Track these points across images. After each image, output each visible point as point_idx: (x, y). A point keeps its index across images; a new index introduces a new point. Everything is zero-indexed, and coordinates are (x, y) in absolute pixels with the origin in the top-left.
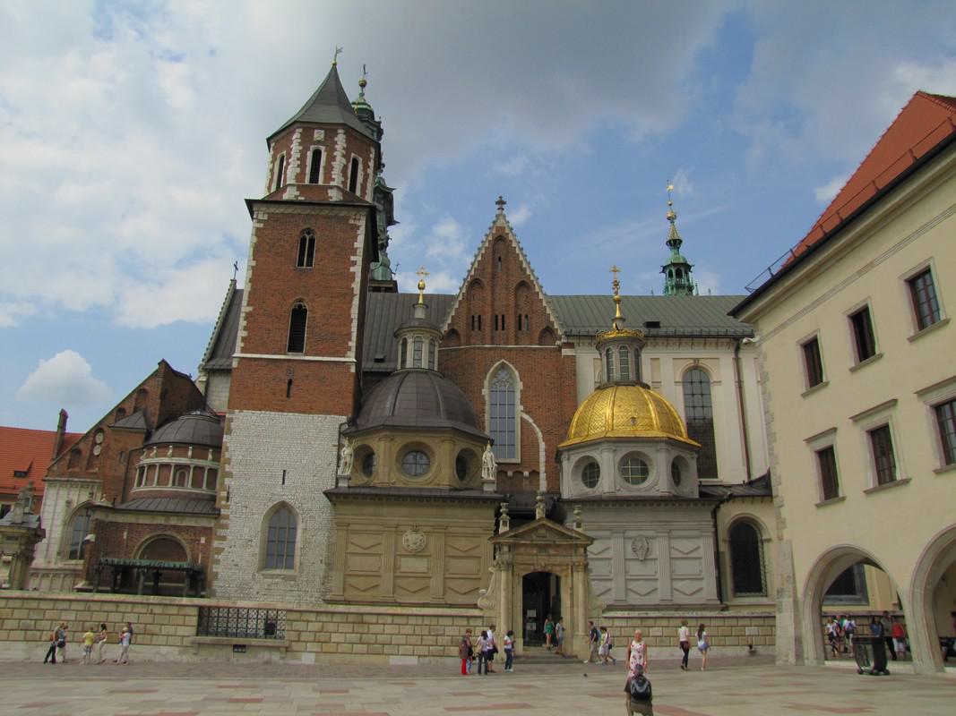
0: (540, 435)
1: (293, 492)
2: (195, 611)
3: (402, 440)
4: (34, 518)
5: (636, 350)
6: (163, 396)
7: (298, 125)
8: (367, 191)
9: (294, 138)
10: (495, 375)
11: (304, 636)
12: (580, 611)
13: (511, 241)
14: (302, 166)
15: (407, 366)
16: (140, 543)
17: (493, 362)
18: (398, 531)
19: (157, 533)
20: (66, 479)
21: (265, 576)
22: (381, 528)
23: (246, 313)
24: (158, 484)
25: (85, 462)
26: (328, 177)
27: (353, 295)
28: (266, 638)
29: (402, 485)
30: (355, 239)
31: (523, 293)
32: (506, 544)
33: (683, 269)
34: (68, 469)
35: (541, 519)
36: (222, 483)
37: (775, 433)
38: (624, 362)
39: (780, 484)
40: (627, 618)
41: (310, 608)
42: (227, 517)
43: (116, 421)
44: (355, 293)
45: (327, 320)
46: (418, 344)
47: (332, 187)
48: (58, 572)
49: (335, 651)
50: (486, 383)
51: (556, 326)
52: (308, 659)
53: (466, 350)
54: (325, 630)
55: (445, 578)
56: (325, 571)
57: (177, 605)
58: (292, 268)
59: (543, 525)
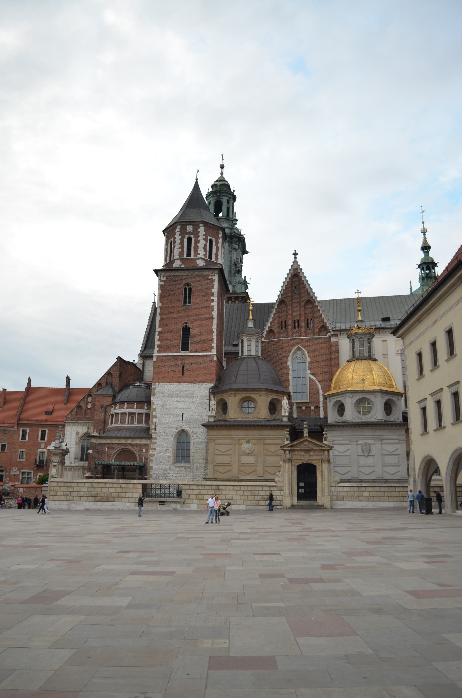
0: (320, 386)
2: (141, 486)
4: (63, 444)
5: (369, 339)
6: (120, 376)
7: (178, 224)
8: (219, 257)
9: (176, 231)
10: (295, 353)
11: (192, 497)
12: (326, 483)
14: (182, 247)
15: (244, 355)
17: (293, 347)
18: (239, 442)
19: (120, 448)
20: (75, 421)
21: (176, 467)
23: (159, 332)
24: (121, 423)
25: (84, 412)
26: (196, 253)
27: (213, 318)
28: (178, 498)
29: (241, 419)
31: (309, 306)
32: (287, 450)
33: (431, 266)
34: (76, 415)
35: (306, 436)
36: (152, 421)
37: (409, 397)
41: (194, 483)
42: (156, 438)
43: (97, 391)
44: (214, 317)
46: (249, 343)
47: (198, 259)
48: (76, 468)
50: (290, 359)
51: (328, 325)
53: (278, 341)
54: (201, 494)
56: (205, 464)
57: (132, 484)
58: (180, 306)
59: (306, 440)
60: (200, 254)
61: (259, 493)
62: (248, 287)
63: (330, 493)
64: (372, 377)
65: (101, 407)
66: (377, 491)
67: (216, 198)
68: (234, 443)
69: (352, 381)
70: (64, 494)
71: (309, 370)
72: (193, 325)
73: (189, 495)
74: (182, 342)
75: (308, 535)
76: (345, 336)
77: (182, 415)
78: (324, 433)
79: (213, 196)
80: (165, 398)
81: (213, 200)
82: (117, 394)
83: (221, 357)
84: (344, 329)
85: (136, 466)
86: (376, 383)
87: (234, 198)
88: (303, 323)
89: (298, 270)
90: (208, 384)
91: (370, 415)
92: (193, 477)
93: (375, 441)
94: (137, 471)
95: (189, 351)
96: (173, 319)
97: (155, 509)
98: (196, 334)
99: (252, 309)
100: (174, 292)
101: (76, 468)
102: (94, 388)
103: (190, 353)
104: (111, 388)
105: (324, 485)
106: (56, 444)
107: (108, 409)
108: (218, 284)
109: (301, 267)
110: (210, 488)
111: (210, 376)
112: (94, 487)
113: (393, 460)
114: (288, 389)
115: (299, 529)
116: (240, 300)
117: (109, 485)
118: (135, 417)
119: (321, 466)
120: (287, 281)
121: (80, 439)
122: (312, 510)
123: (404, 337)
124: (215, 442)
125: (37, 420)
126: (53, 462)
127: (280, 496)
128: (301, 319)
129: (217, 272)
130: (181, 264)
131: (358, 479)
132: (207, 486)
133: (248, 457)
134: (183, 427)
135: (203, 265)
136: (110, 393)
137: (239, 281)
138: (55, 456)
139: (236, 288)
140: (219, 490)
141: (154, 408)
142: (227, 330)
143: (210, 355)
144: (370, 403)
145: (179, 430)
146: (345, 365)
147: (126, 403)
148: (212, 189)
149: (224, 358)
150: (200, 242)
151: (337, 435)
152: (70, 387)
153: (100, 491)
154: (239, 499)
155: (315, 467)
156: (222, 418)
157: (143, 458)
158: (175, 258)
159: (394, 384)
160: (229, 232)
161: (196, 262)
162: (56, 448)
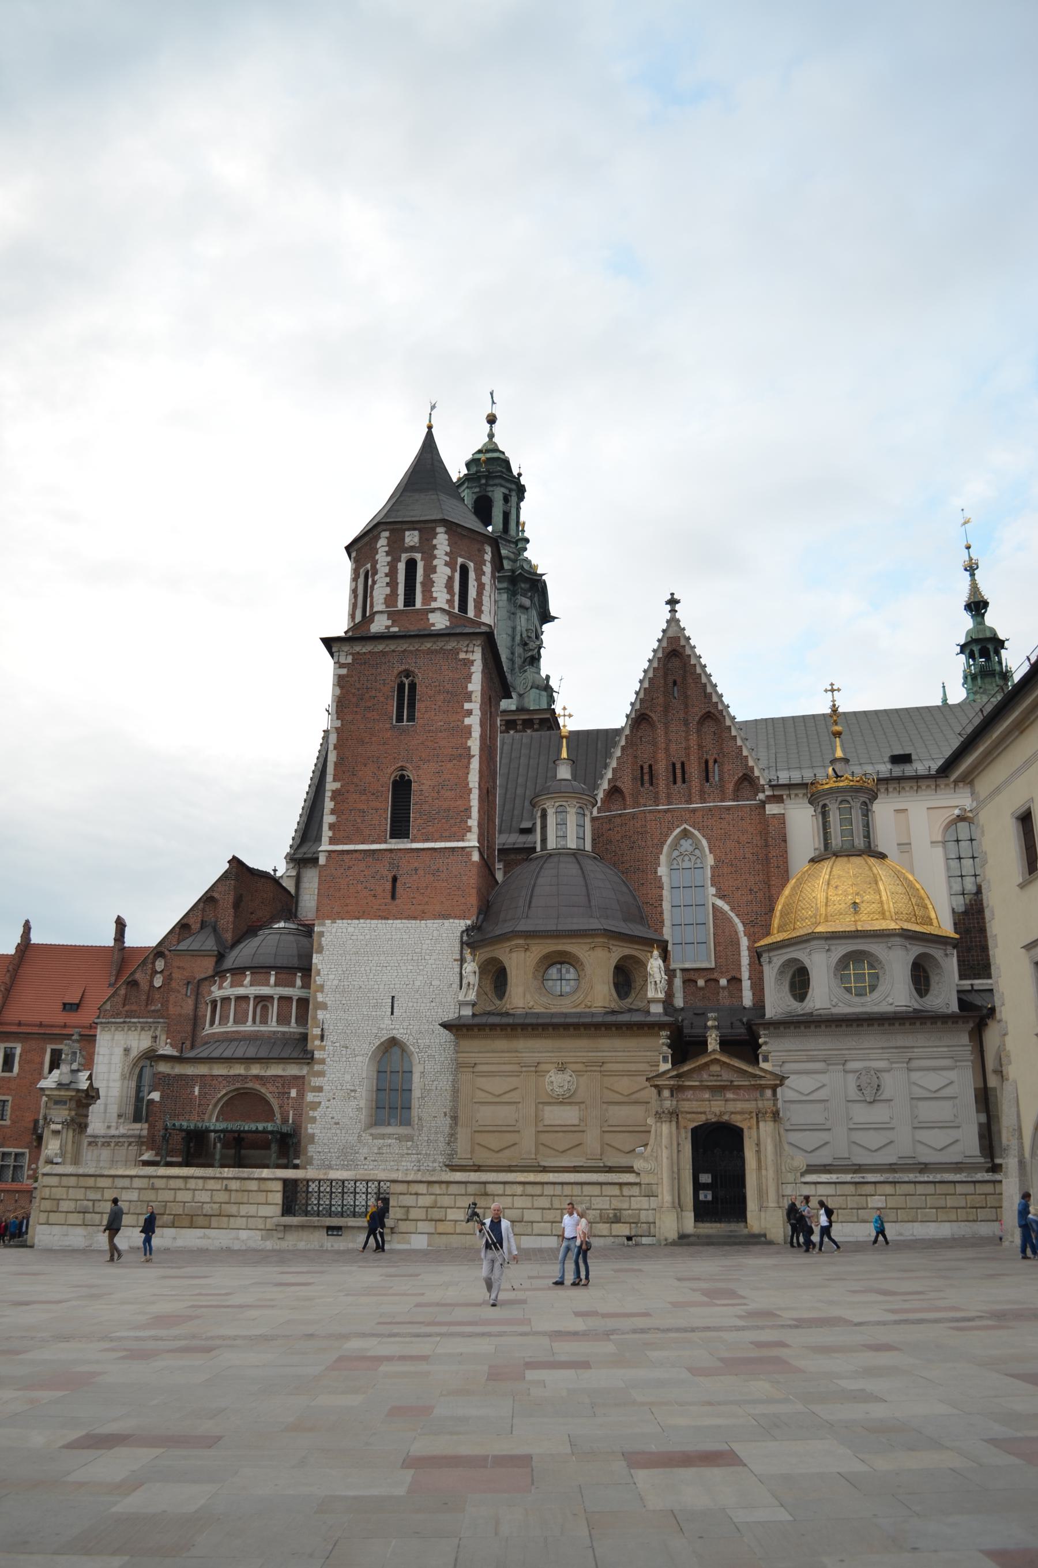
0: (740, 928)
1: (406, 1024)
2: (278, 1186)
3: (540, 949)
4: (84, 1075)
5: (865, 803)
6: (237, 905)
7: (382, 527)
8: (483, 608)
10: (675, 846)
11: (414, 1214)
12: (770, 1174)
13: (689, 656)
14: (393, 584)
17: (671, 830)
18: (538, 1071)
19: (232, 1087)
20: (121, 1020)
21: (374, 1137)
22: (516, 1068)
23: (333, 791)
24: (235, 1022)
25: (144, 997)
26: (429, 597)
27: (470, 757)
29: (543, 1010)
30: (468, 678)
31: (709, 728)
32: (666, 1087)
33: (991, 647)
34: (124, 1005)
35: (714, 1050)
36: (315, 1018)
37: (996, 935)
39: (1003, 1004)
40: (835, 1183)
41: (419, 1177)
42: (323, 1062)
43: (179, 943)
44: (472, 753)
46: (560, 817)
47: (433, 610)
48: (121, 1140)
49: (452, 1231)
50: (663, 858)
51: (757, 773)
52: (419, 1242)
53: (633, 816)
54: (438, 1205)
56: (451, 1127)
57: (256, 1179)
58: (388, 726)
59: (716, 1059)
60: (438, 600)
61: (593, 1202)
62: (554, 701)
63: (781, 1200)
64: (878, 897)
65: (185, 982)
66: (906, 1195)
67: (477, 490)
68: (525, 1072)
69: (826, 910)
70: (76, 1208)
71: (712, 886)
72: (420, 772)
73: (408, 1208)
74: (392, 817)
75: (782, 1344)
76: (801, 801)
78: (761, 1041)
80: (348, 958)
81: (470, 494)
82: (227, 951)
83: (491, 854)
84: (799, 781)
85: (272, 1132)
86: (887, 914)
87: (521, 490)
88: (694, 771)
90: (457, 921)
91: (875, 995)
92: (419, 1161)
93: (892, 1063)
94: (274, 1147)
96: (369, 758)
97: (317, 1247)
98: (427, 795)
100: (373, 693)
101: (121, 1140)
102: (170, 936)
104: (212, 934)
105: (764, 1180)
106: (60, 1074)
107: (204, 989)
108: (483, 672)
109: (687, 633)
110: (461, 1189)
111: (463, 900)
112: (157, 1189)
113: (941, 1111)
114: (661, 934)
115: (740, 1317)
117: (196, 1184)
119: (755, 1130)
122: (736, 1247)
123: (975, 777)
124: (476, 1070)
125: (41, 1025)
126: (53, 1122)
127: (647, 1210)
129: (479, 642)
131: (850, 1163)
132: (454, 1185)
133: (562, 1108)
134: (394, 1032)
135: (444, 627)
136: (209, 948)
137: (533, 683)
138: (55, 1107)
139: (526, 700)
140: (486, 1194)
141: (318, 983)
142: (506, 794)
144: (875, 964)
145: (382, 1040)
146: (807, 871)
147: (248, 973)
148: (468, 469)
149: (499, 861)
151: (794, 1047)
152: (124, 943)
153: (172, 1200)
154: (540, 1220)
156: (494, 1007)
157: (291, 1112)
158: (375, 609)
159: (933, 915)
160: (510, 568)
161: (428, 619)
162: (61, 1086)
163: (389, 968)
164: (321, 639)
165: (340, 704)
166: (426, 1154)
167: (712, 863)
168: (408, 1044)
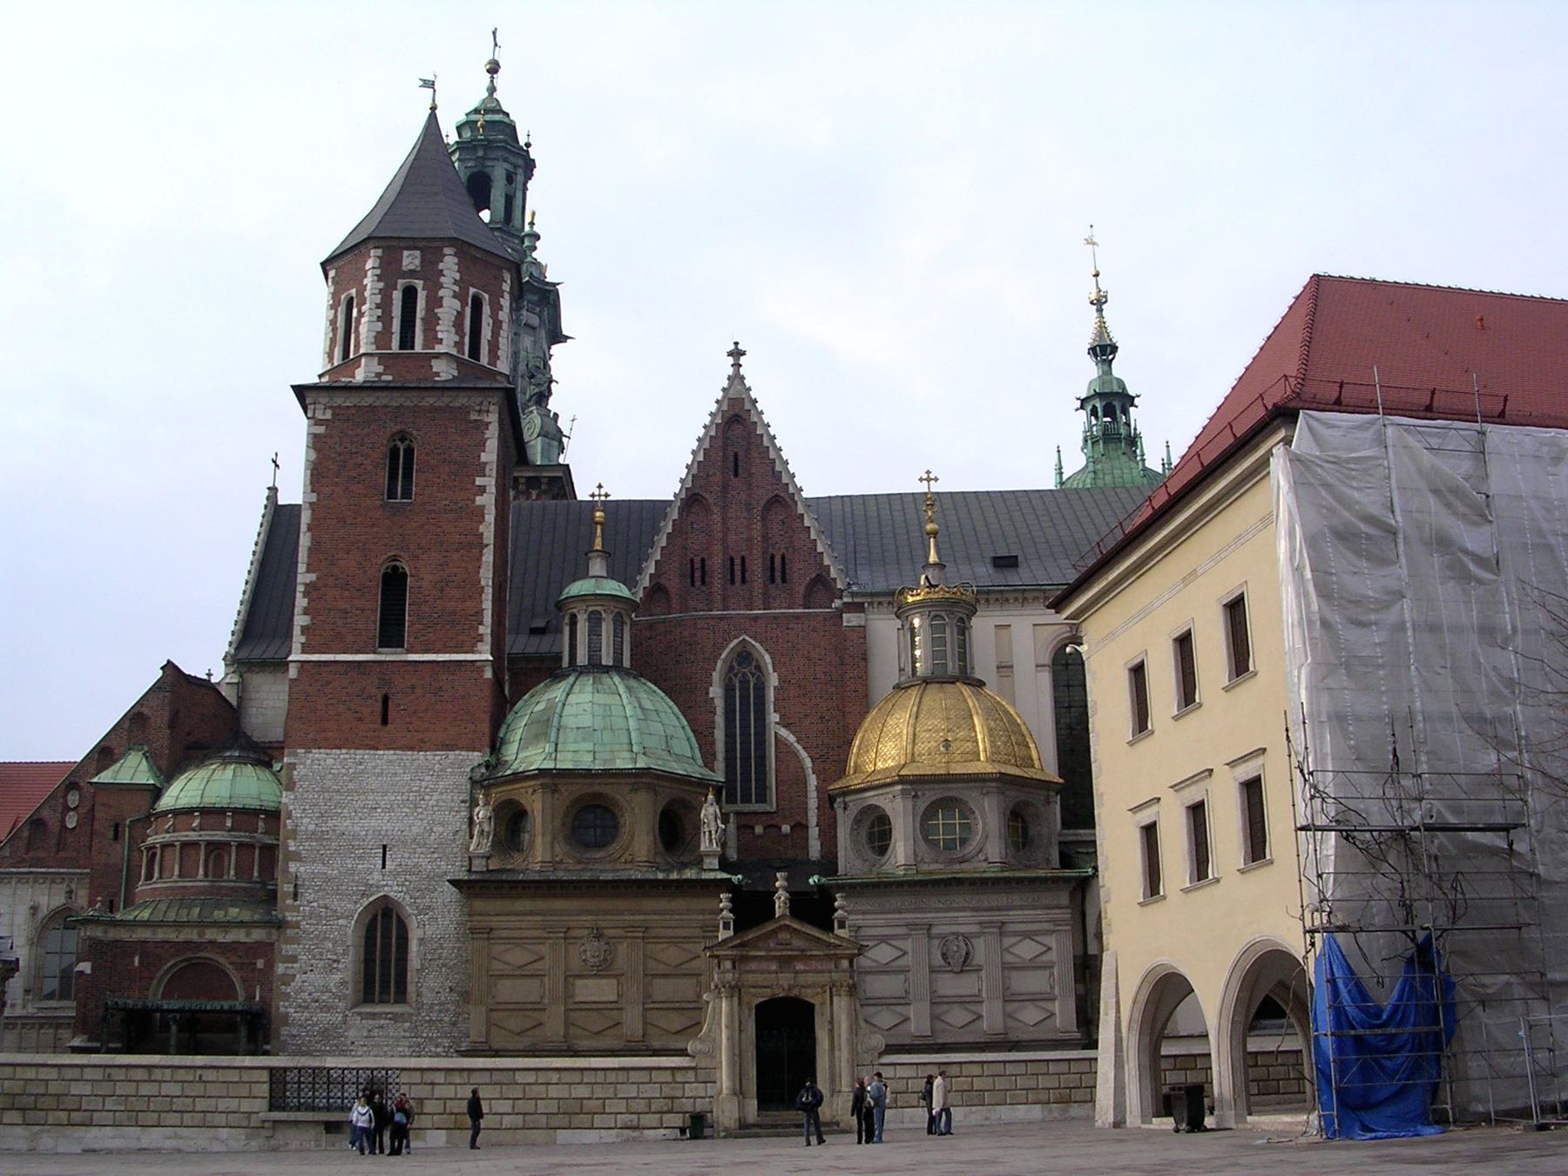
0: (808, 763)
2: (265, 1076)
5: (961, 619)
6: (173, 724)
8: (499, 353)
11: (430, 1106)
12: (843, 1056)
14: (385, 318)
16: (162, 972)
23: (306, 585)
26: (432, 338)
30: (482, 446)
32: (727, 957)
34: (28, 851)
35: (783, 916)
36: (286, 871)
38: (937, 642)
42: (297, 925)
44: (485, 542)
45: (442, 590)
51: (833, 574)
53: (680, 622)
55: (645, 1009)
60: (444, 342)
71: (775, 711)
74: (382, 619)
77: (381, 851)
79: (462, 157)
87: (530, 166)
88: (757, 569)
89: (743, 404)
92: (419, 1046)
94: (243, 1031)
95: (402, 646)
99: (602, 520)
103: (408, 653)
109: (753, 395)
116: (543, 487)
118: (226, 858)
119: (828, 1006)
120: (711, 437)
121: (43, 927)
124: (491, 936)
128: (751, 554)
129: (495, 400)
130: (381, 371)
135: (451, 377)
141: (289, 827)
143: (472, 662)
145: (371, 899)
150: (446, 302)
155: (810, 1008)
161: (431, 367)
163: (379, 810)
164: (292, 386)
165: (316, 472)
166: (427, 1037)
167: (777, 684)
168: (404, 904)
